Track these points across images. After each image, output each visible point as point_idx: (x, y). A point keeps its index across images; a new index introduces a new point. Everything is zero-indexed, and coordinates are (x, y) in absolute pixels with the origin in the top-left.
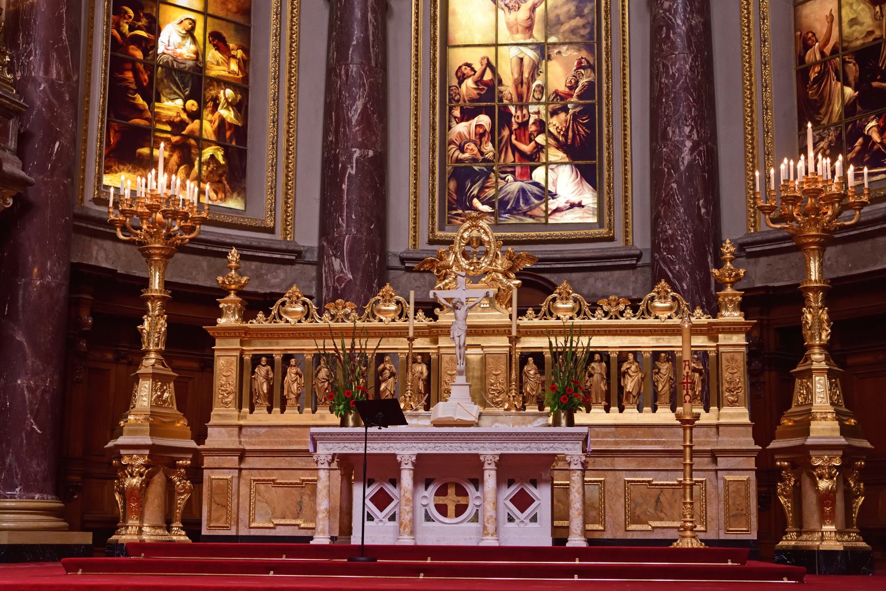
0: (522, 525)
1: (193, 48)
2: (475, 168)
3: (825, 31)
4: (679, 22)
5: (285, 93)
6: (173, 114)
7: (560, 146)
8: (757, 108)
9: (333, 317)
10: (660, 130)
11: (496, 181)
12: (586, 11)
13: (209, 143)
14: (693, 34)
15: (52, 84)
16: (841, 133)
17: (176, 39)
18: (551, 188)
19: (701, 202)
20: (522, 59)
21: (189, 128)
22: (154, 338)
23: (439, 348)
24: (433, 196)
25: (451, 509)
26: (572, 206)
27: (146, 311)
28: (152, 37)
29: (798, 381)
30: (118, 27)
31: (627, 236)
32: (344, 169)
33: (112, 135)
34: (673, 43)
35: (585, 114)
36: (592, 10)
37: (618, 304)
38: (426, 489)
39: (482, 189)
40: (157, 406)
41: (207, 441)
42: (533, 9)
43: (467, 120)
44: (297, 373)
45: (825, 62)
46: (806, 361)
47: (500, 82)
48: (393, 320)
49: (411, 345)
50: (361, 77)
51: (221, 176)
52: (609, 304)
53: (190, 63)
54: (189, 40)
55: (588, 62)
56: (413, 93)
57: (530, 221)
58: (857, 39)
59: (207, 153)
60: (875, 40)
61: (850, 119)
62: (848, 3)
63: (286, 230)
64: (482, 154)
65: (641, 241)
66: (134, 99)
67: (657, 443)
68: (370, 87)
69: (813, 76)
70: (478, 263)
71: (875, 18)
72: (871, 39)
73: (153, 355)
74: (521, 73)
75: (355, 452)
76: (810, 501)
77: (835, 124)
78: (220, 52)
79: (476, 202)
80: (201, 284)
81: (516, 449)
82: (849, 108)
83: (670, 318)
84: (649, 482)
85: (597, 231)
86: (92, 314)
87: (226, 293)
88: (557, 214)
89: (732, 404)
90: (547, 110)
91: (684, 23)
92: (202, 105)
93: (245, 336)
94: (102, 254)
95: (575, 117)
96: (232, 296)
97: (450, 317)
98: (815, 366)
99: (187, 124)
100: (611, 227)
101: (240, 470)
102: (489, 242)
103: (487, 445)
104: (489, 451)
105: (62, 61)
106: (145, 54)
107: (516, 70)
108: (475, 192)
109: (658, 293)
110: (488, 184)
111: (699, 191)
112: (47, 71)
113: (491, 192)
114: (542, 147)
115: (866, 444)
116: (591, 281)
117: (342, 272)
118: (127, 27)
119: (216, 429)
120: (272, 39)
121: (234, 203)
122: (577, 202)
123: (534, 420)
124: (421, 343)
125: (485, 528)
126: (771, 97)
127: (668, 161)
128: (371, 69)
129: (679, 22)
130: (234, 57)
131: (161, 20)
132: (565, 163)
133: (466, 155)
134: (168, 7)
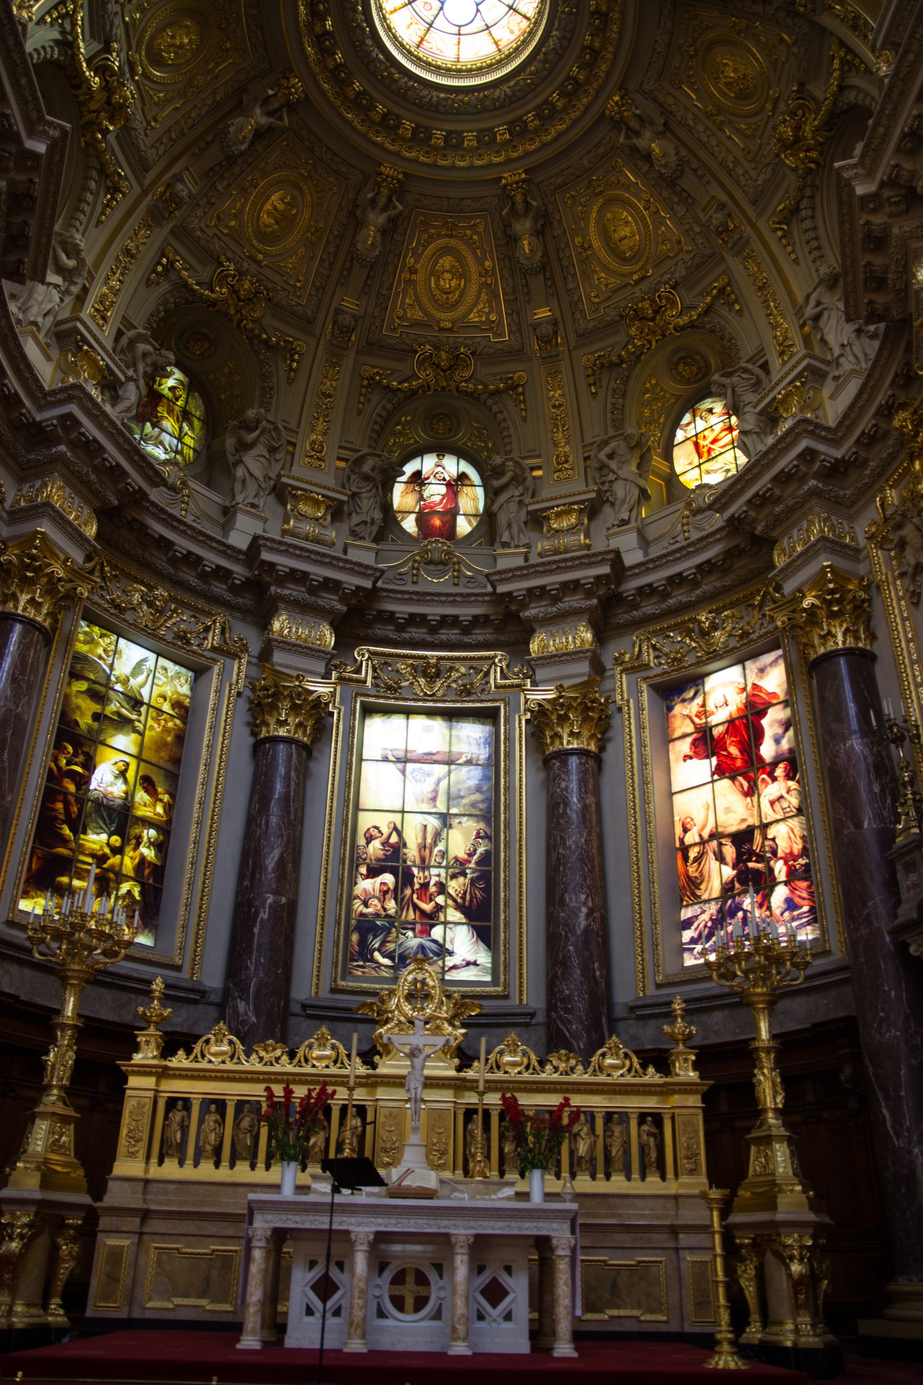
0: (494, 1325)
1: (124, 787)
2: (379, 923)
6: (96, 847)
7: (459, 907)
9: (261, 1059)
10: (557, 896)
13: (128, 878)
17: (109, 778)
18: (448, 946)
19: (596, 965)
23: (377, 1100)
24: (338, 946)
25: (409, 1301)
26: (468, 964)
27: (53, 1040)
28: (87, 773)
29: (753, 1149)
30: (56, 760)
32: (257, 913)
33: (34, 860)
34: (569, 818)
36: (490, 788)
37: (568, 1060)
38: (380, 1274)
39: (383, 943)
40: (53, 1151)
41: (106, 1198)
42: (438, 783)
43: (373, 877)
44: (216, 1121)
46: (761, 1126)
47: (405, 845)
48: (327, 1067)
49: (351, 1095)
50: (280, 828)
52: (559, 1059)
53: (120, 801)
54: (121, 780)
56: (325, 848)
59: (125, 887)
63: (193, 969)
64: (385, 909)
67: (612, 1216)
68: (288, 839)
70: (423, 1009)
72: (743, 826)
73: (55, 1092)
74: (425, 838)
75: (300, 1226)
76: (781, 1289)
78: (149, 794)
79: (377, 955)
80: (104, 1017)
81: (493, 1228)
83: (622, 1075)
84: (604, 1261)
85: (492, 989)
89: (692, 1172)
92: (125, 841)
95: (473, 882)
96: (152, 1030)
97: (406, 1066)
98: (774, 1132)
101: (141, 1234)
102: (434, 987)
103: (459, 1223)
104: (462, 1231)
106: (78, 788)
107: (420, 835)
108: (377, 946)
109: (610, 1048)
115: (827, 1220)
117: (246, 1014)
118: (64, 761)
119: (118, 1183)
120: (199, 787)
121: (145, 940)
123: (499, 1190)
124: (360, 1094)
125: (454, 1330)
129: (575, 800)
130: (161, 800)
131: (97, 759)
132: (463, 924)
133: (370, 910)
134: (105, 748)
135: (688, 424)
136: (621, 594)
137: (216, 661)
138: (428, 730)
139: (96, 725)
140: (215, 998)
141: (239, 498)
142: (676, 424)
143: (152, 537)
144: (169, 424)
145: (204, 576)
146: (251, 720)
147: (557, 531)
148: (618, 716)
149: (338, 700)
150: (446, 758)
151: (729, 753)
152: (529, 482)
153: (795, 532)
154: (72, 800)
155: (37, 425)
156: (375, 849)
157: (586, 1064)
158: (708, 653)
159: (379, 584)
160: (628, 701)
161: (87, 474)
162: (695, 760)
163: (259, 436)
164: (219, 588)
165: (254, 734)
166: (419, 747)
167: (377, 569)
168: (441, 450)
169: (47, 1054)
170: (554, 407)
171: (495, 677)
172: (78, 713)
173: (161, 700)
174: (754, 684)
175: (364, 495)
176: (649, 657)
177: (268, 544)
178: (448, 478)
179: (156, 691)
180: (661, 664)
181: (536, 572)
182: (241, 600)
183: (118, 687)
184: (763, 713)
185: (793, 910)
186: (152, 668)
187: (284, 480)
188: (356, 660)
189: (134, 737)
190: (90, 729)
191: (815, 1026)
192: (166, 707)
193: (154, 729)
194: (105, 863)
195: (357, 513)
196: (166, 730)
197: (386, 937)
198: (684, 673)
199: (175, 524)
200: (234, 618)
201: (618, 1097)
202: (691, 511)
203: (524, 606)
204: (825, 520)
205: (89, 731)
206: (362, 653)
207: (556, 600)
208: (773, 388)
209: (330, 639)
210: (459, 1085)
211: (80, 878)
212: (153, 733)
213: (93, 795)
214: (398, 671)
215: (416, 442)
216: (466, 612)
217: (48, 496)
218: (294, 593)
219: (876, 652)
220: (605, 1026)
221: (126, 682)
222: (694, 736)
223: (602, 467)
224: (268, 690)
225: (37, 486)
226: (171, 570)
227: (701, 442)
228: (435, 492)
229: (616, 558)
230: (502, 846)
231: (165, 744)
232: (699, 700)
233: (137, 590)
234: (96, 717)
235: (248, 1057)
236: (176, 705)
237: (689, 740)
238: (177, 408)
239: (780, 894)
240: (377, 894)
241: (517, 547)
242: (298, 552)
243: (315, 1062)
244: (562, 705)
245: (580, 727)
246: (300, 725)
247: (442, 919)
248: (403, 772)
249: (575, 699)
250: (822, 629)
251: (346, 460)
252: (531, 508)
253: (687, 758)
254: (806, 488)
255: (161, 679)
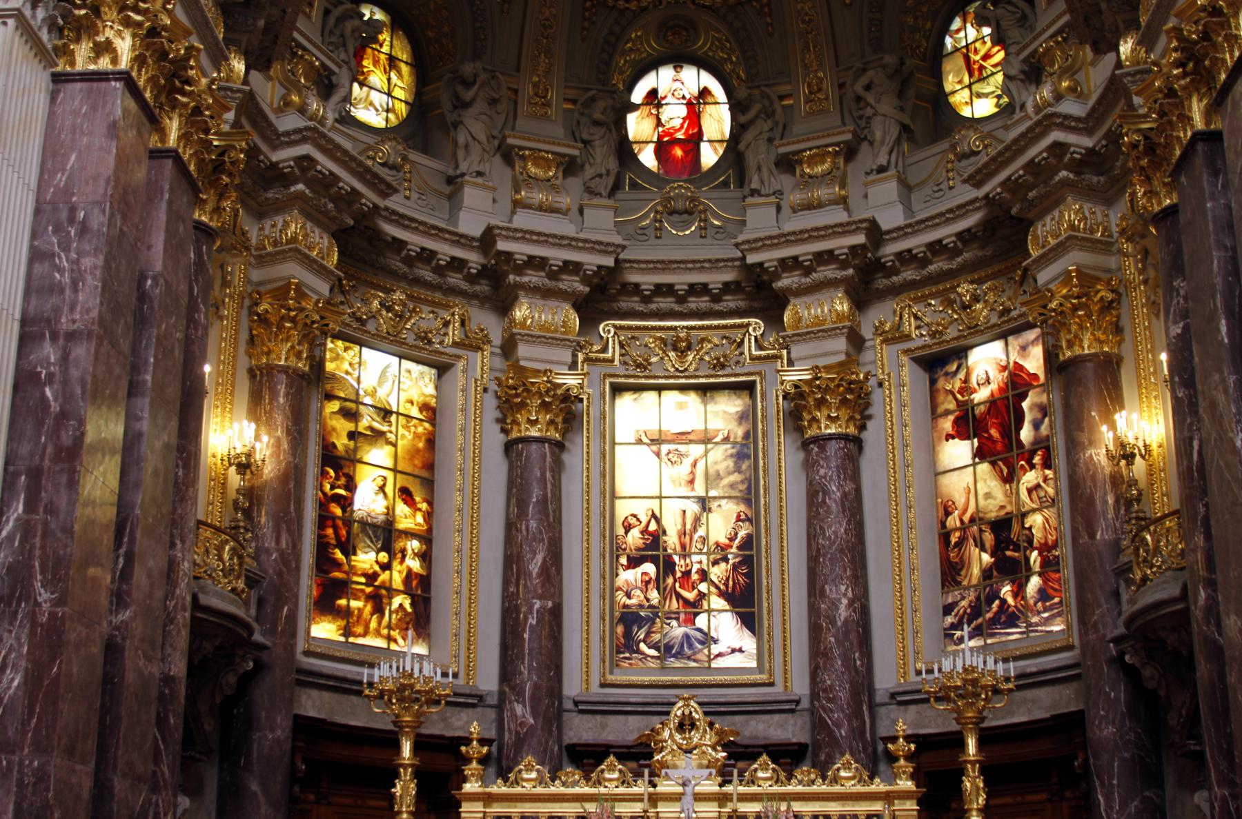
1: (385, 503)
2: (642, 614)
3: (963, 500)
4: (834, 488)
5: (467, 545)
6: (367, 566)
7: (722, 594)
8: (906, 570)
10: (818, 587)
11: (662, 627)
12: (744, 467)
13: (399, 592)
14: (847, 499)
15: (282, 554)
16: (979, 595)
18: (713, 634)
19: (857, 655)
20: (684, 511)
21: (381, 579)
22: (408, 800)
23: (658, 812)
24: (604, 641)
26: (733, 651)
27: (397, 776)
28: (349, 494)
30: (322, 486)
31: (786, 682)
32: (526, 619)
34: (829, 507)
35: (745, 564)
36: (750, 466)
37: (809, 773)
39: (648, 634)
42: (694, 464)
43: (634, 568)
45: (964, 529)
47: (664, 532)
48: (617, 787)
50: (541, 532)
51: (408, 623)
53: (382, 518)
54: (381, 495)
55: (746, 515)
57: (694, 664)
58: (991, 511)
59: (397, 601)
60: (1007, 514)
61: (987, 582)
62: (982, 479)
64: (648, 600)
65: (800, 687)
66: (334, 554)
69: (953, 540)
71: (1006, 494)
72: (1003, 513)
74: (684, 524)
77: (974, 586)
79: (643, 646)
82: (987, 573)
85: (758, 677)
86: (304, 761)
87: (469, 761)
88: (719, 658)
90: (708, 559)
91: (838, 490)
93: (488, 799)
94: (310, 703)
95: (735, 567)
96: (474, 764)
99: (379, 575)
100: (771, 674)
102: (699, 720)
105: (290, 532)
106: (344, 511)
107: (679, 521)
108: (642, 637)
110: (654, 629)
111: (855, 644)
112: (278, 542)
113: (656, 637)
114: (705, 594)
116: (753, 723)
117: (524, 716)
118: (328, 486)
122: (738, 648)
126: (917, 559)
127: (828, 617)
128: (549, 525)
129: (834, 488)
131: (358, 478)
132: (726, 611)
135: (958, 31)
136: (880, 259)
137: (459, 357)
138: (681, 406)
139: (352, 444)
140: (493, 700)
141: (463, 167)
142: (944, 30)
143: (385, 241)
144: (377, 78)
145: (439, 270)
146: (499, 415)
147: (811, 177)
148: (878, 391)
149: (586, 383)
150: (701, 436)
151: (990, 435)
152: (779, 114)
153: (1048, 219)
154: (340, 523)
155: (274, 166)
156: (634, 538)
157: (824, 778)
158: (970, 328)
159: (622, 256)
160: (889, 375)
161: (325, 205)
162: (956, 440)
163: (477, 93)
164: (455, 279)
165: (504, 431)
166: (674, 425)
167: (618, 246)
168: (678, 61)
169: (394, 786)
170: (803, 21)
171: (750, 348)
172: (335, 434)
173: (409, 405)
174: (1016, 363)
175: (597, 143)
176: (909, 326)
177: (504, 233)
178: (688, 97)
179: (404, 396)
180: (922, 335)
181: (787, 241)
182: (478, 288)
183: (368, 400)
184: (1024, 396)
185: (1046, 601)
186: (397, 374)
187: (510, 141)
188: (602, 337)
189: (390, 449)
190: (347, 450)
191: (1054, 717)
192: (415, 412)
193: (406, 436)
194: (376, 580)
195: (591, 165)
196: (417, 436)
197: (650, 628)
198: (945, 347)
199: (406, 222)
200: (471, 306)
201: (850, 803)
202: (956, 155)
203: (776, 276)
204: (1076, 213)
205: (347, 452)
206: (606, 328)
207: (808, 271)
208: (1035, 39)
209: (574, 320)
210: (723, 799)
211: (357, 598)
212: (405, 442)
213: (358, 515)
214: (646, 346)
215: (649, 54)
216: (716, 279)
217: (294, 239)
218: (534, 279)
219: (1124, 354)
220: (866, 713)
221: (373, 393)
222: (957, 413)
223: (858, 99)
224: (516, 389)
225: (279, 227)
226: (406, 269)
227: (972, 56)
228: (674, 114)
229: (873, 229)
230: (763, 531)
231: (418, 451)
232: (962, 375)
233: (376, 297)
234: (352, 435)
235: (553, 781)
236: (424, 407)
237: (951, 418)
238: (383, 57)
239: (1034, 583)
240: (639, 584)
241: (767, 195)
242: (535, 237)
243: (606, 784)
244: (819, 387)
245: (838, 409)
246: (551, 422)
247: (705, 604)
248: (658, 454)
249: (832, 380)
250: (1069, 331)
251: (574, 102)
252: (782, 150)
253: (949, 437)
254: (1057, 178)
255: (406, 383)
